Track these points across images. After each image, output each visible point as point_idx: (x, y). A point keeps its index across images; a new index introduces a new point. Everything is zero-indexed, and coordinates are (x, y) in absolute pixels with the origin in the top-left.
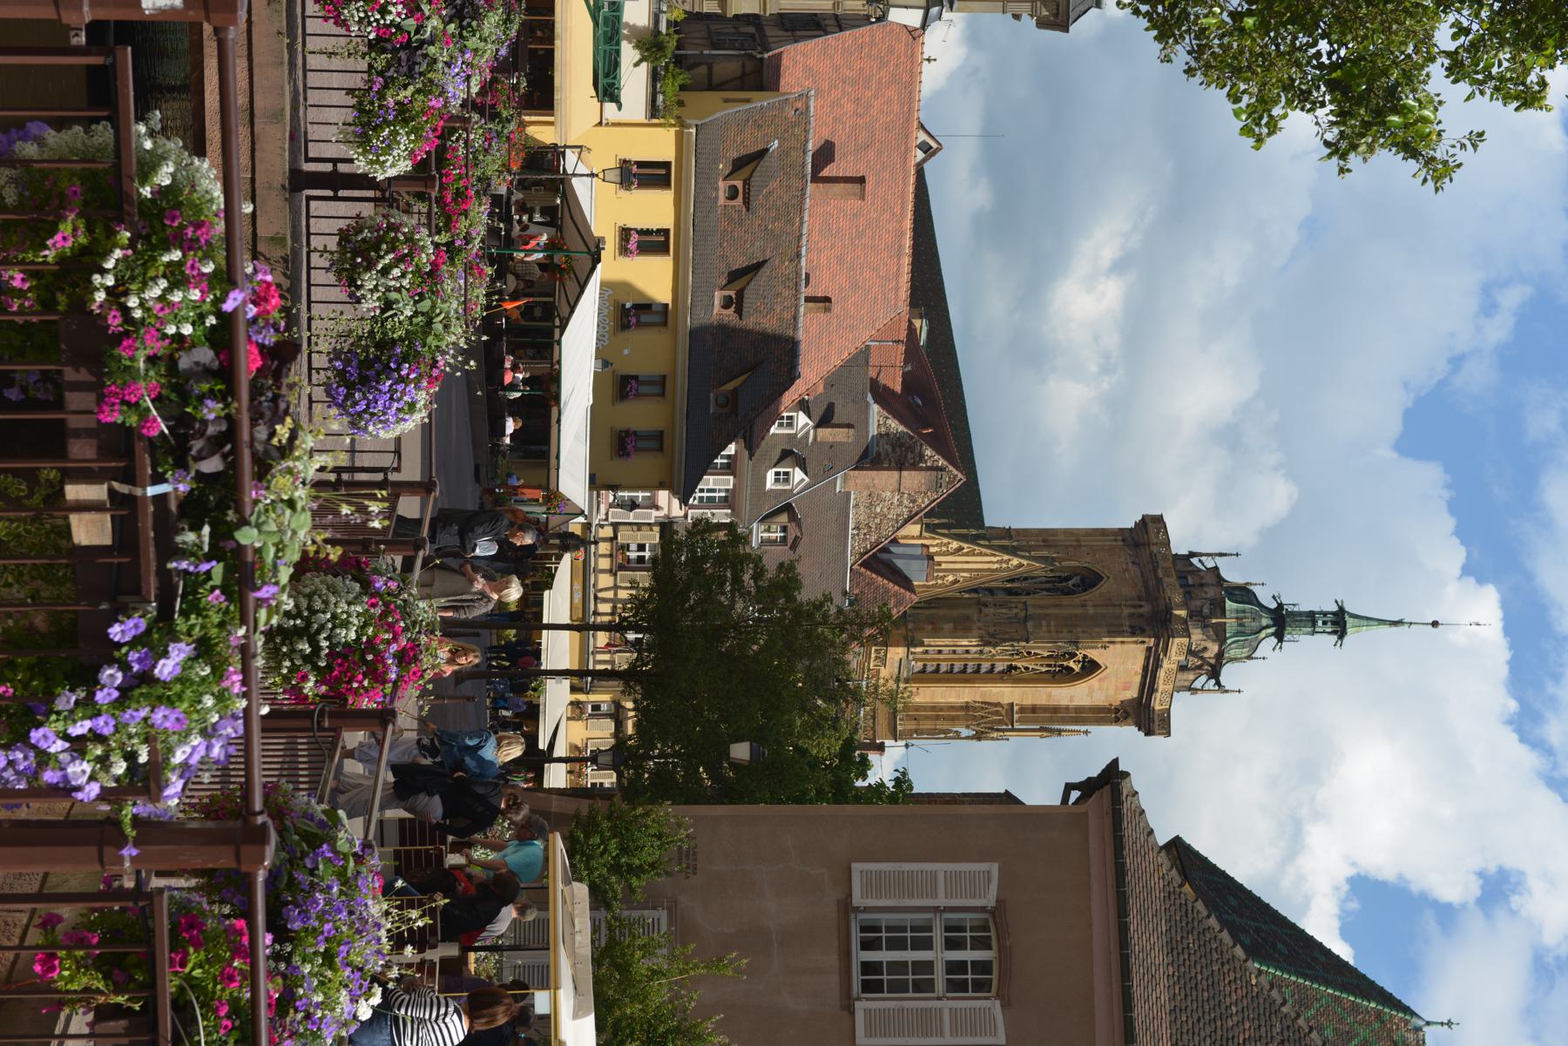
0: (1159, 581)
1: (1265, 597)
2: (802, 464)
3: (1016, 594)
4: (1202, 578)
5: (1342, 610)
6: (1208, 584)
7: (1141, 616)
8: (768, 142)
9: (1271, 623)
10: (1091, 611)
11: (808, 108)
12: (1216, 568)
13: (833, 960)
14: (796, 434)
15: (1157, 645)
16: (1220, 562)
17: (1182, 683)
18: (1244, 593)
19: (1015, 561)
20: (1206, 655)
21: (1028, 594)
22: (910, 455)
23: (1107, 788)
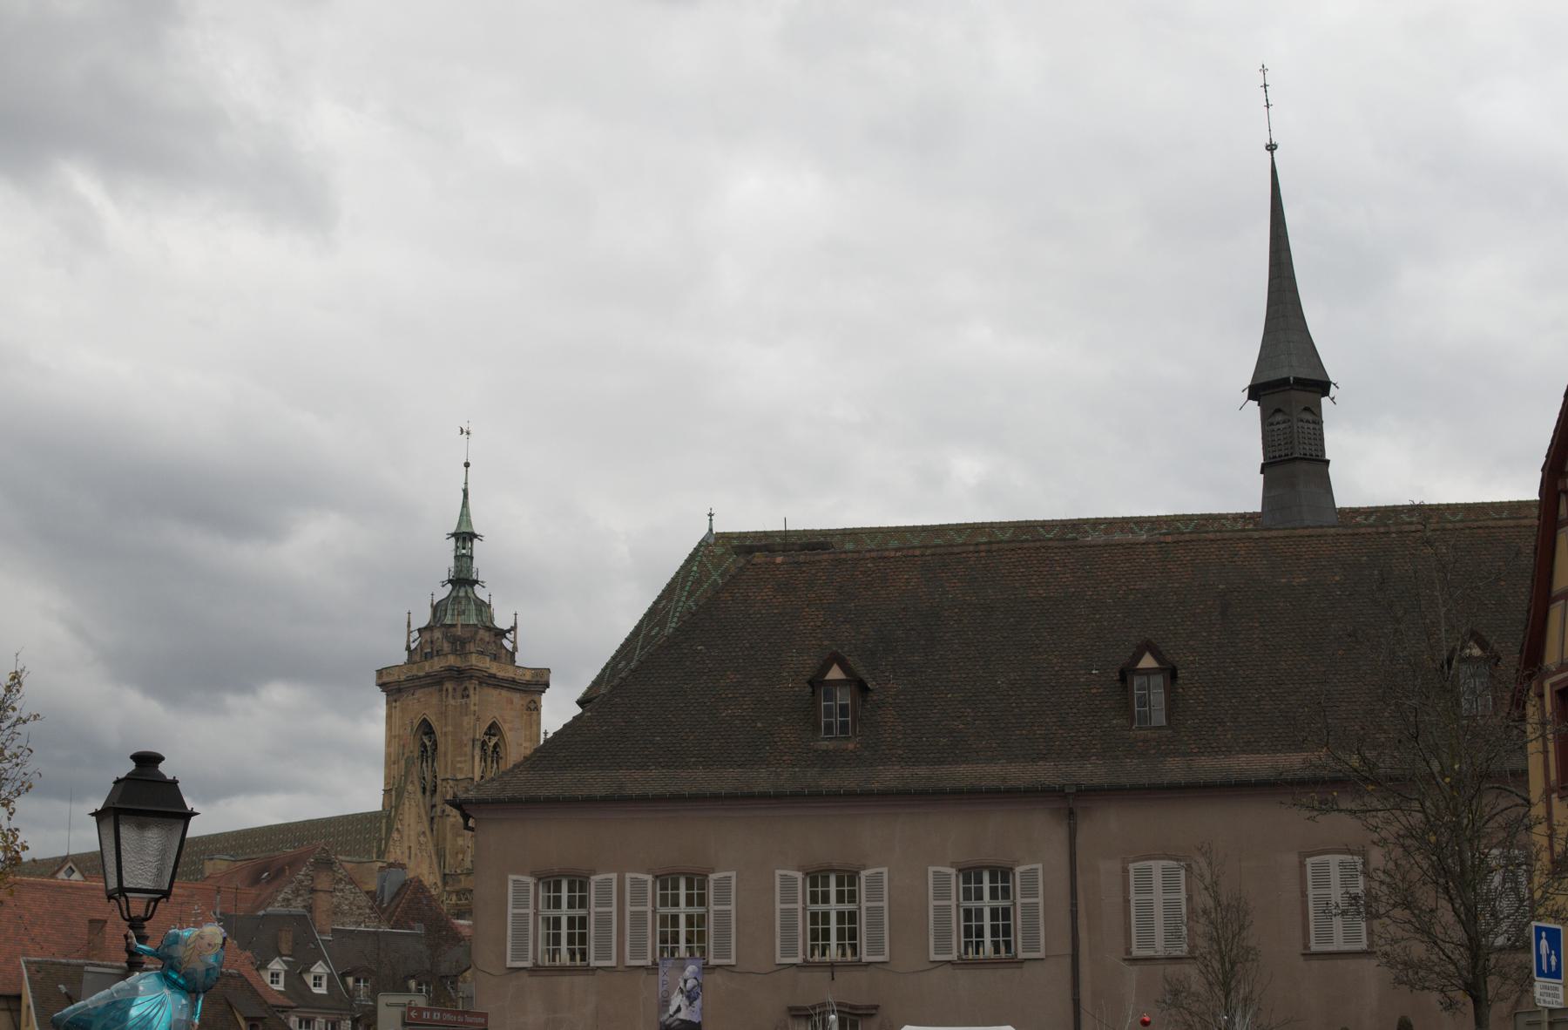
0: (428, 675)
1: (444, 592)
2: (307, 970)
3: (435, 787)
4: (426, 641)
5: (453, 535)
6: (431, 637)
7: (454, 689)
8: (60, 993)
10: (450, 728)
11: (35, 962)
12: (420, 630)
13: (565, 980)
14: (286, 971)
16: (414, 627)
17: (509, 659)
18: (437, 609)
19: (410, 788)
20: (487, 639)
21: (436, 777)
22: (306, 883)
23: (464, 806)
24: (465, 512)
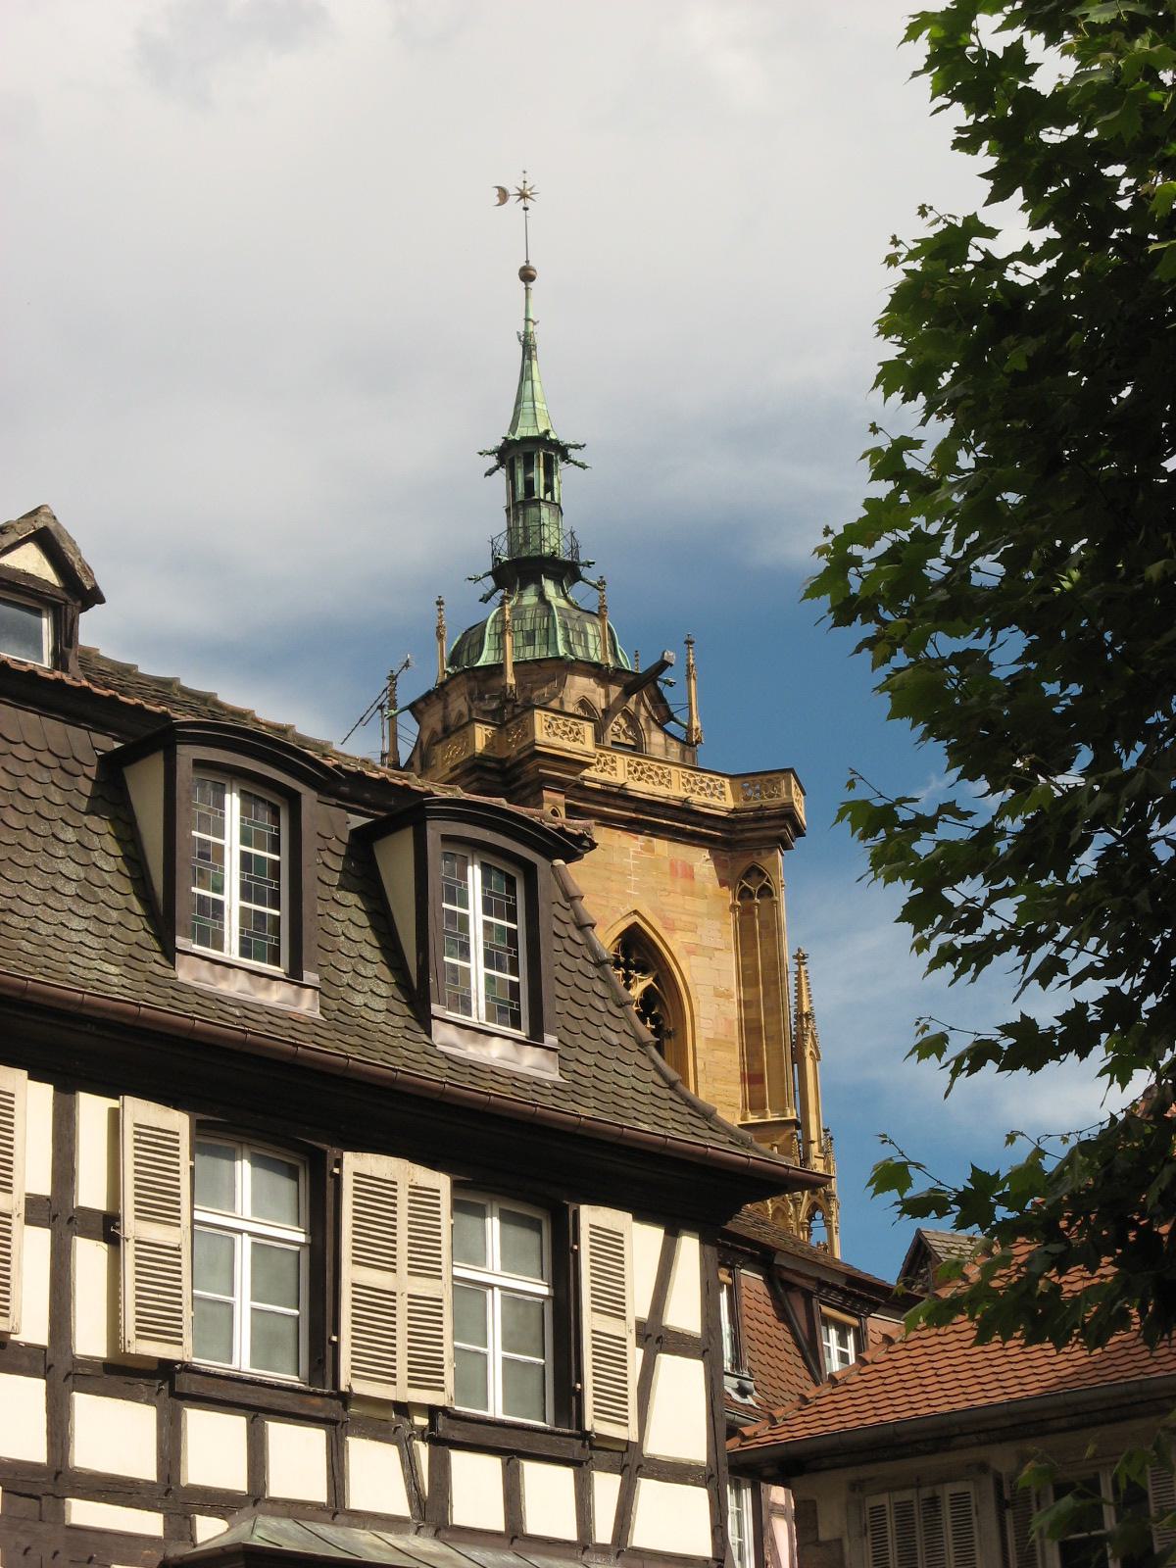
6: (445, 718)
9: (532, 589)
15: (560, 785)
20: (600, 702)
24: (527, 392)
